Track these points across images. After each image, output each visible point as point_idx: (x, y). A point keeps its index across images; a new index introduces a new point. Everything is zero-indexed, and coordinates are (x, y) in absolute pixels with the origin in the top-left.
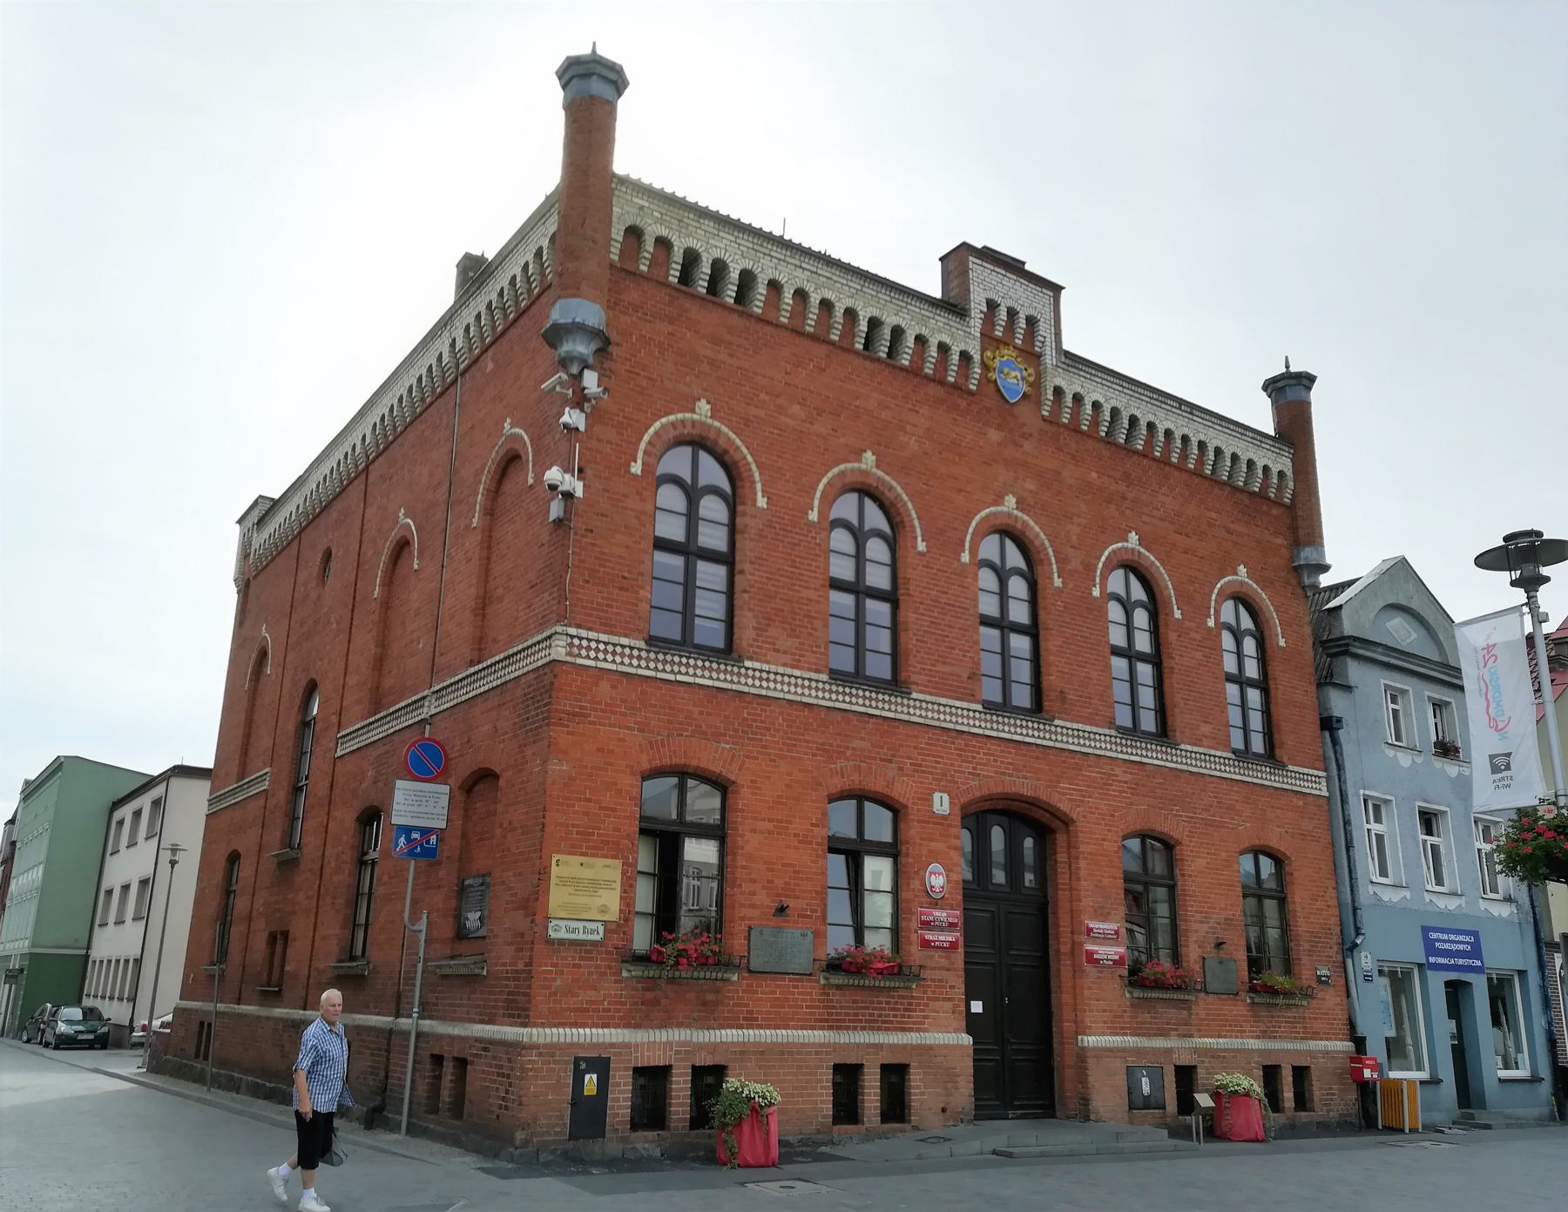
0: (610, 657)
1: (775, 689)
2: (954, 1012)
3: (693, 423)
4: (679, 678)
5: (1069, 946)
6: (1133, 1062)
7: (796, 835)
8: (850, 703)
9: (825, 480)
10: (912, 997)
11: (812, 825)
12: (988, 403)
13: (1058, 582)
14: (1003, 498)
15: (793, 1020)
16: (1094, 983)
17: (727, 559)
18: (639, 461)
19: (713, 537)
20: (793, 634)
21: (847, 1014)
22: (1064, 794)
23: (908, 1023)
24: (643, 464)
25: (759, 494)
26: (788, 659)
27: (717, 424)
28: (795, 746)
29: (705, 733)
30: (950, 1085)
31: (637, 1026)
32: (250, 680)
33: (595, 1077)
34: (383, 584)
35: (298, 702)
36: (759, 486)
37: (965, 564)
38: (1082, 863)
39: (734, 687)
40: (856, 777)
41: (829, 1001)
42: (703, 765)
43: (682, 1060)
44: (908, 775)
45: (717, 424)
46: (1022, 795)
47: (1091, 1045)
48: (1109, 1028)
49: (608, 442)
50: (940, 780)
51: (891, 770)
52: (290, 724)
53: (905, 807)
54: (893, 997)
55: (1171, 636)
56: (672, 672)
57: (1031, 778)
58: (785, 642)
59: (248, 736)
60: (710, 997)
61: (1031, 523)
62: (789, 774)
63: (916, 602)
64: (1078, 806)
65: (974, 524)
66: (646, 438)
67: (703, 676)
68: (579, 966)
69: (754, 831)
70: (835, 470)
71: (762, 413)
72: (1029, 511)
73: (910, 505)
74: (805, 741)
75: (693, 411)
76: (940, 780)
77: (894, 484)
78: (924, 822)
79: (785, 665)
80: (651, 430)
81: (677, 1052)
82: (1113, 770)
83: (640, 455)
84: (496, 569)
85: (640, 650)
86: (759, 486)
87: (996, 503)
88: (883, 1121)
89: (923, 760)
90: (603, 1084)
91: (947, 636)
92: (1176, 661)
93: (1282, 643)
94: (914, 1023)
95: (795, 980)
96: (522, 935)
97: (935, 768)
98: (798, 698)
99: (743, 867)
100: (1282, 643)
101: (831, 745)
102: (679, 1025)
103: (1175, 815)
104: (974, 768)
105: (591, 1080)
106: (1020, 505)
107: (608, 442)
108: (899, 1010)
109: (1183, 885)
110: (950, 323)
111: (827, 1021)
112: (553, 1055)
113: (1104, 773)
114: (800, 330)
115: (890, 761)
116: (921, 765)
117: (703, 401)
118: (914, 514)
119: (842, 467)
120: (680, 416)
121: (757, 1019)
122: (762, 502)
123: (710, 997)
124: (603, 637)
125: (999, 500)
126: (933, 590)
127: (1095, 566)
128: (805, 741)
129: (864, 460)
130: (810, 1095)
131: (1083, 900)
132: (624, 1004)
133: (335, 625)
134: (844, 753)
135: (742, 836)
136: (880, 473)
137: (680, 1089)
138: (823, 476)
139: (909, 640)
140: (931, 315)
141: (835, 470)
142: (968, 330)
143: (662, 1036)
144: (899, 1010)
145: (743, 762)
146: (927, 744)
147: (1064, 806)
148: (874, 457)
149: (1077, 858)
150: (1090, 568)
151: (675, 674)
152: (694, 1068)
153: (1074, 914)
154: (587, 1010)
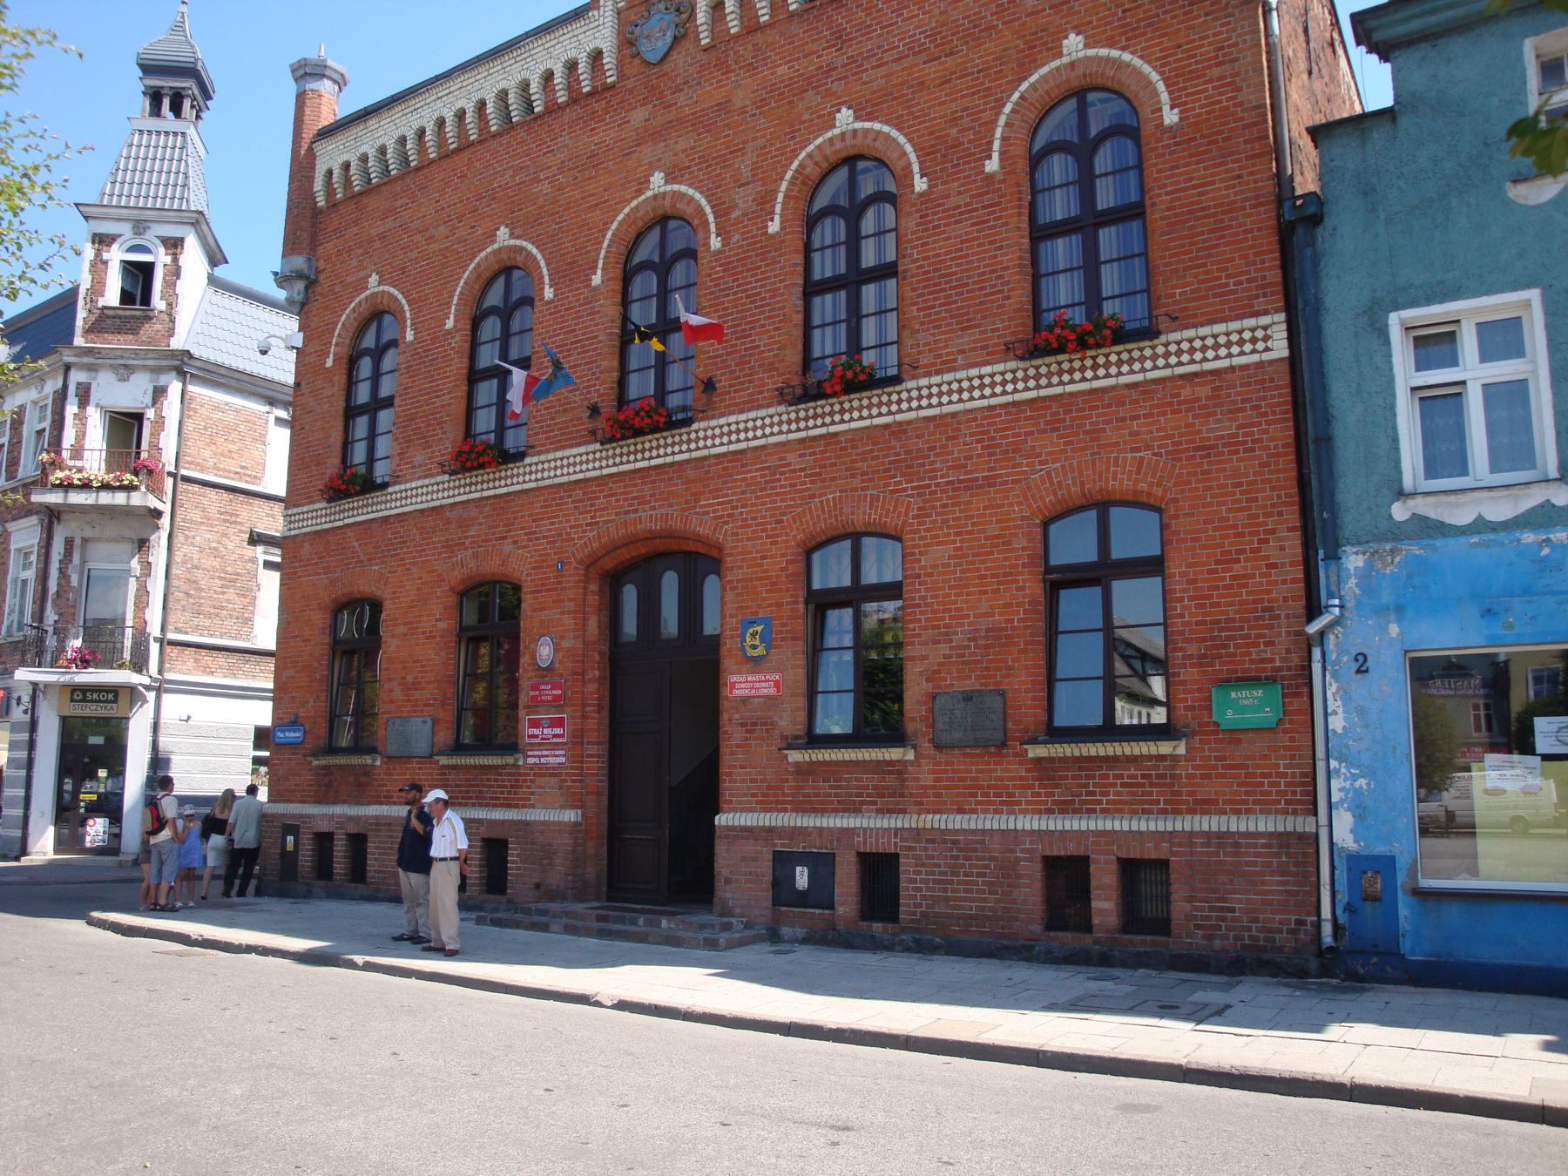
2: (561, 788)
6: (783, 845)
7: (424, 633)
11: (437, 620)
13: (715, 243)
16: (737, 746)
21: (461, 792)
22: (707, 513)
23: (513, 799)
30: (545, 862)
37: (596, 288)
40: (473, 565)
46: (651, 531)
47: (724, 823)
48: (758, 802)
50: (555, 542)
51: (508, 547)
54: (501, 774)
60: (363, 779)
62: (420, 578)
64: (727, 523)
69: (393, 637)
76: (555, 542)
79: (419, 478)
82: (781, 459)
87: (640, 192)
89: (537, 526)
94: (520, 799)
95: (421, 763)
97: (550, 530)
100: (1170, 117)
103: (892, 492)
104: (592, 518)
105: (290, 839)
106: (670, 178)
108: (506, 786)
109: (796, 603)
113: (769, 468)
116: (535, 532)
118: (542, 263)
123: (363, 779)
134: (464, 543)
138: (460, 278)
143: (339, 809)
144: (506, 786)
146: (542, 507)
147: (704, 530)
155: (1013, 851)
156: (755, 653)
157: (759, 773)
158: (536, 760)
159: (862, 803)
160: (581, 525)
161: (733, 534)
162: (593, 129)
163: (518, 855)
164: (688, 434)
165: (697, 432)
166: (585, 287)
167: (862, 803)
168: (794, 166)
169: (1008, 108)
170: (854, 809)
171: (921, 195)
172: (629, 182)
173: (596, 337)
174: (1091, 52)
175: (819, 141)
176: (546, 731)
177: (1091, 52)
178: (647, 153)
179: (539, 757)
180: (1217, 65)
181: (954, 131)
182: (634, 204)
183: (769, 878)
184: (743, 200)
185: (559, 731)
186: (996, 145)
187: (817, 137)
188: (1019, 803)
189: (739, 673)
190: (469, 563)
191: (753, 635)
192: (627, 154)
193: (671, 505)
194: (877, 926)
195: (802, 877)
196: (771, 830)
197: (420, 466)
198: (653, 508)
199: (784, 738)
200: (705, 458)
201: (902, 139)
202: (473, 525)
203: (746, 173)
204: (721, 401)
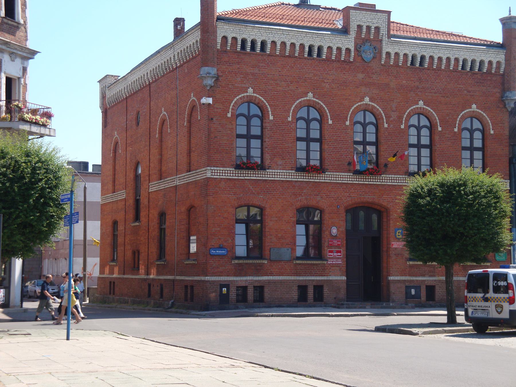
0: (224, 174)
1: (277, 177)
2: (340, 270)
3: (247, 96)
4: (246, 178)
5: (386, 249)
8: (303, 178)
9: (294, 106)
10: (325, 266)
11: (290, 217)
12: (358, 64)
13: (386, 125)
14: (364, 98)
15: (285, 273)
17: (261, 137)
18: (230, 113)
19: (256, 131)
20: (283, 159)
22: (385, 199)
24: (231, 113)
25: (270, 115)
26: (280, 167)
27: (255, 95)
28: (284, 194)
29: (254, 193)
30: (337, 291)
31: (237, 276)
32: (113, 153)
33: (226, 289)
34: (159, 133)
35: (133, 167)
36: (270, 113)
37: (347, 126)
38: (391, 222)
39: (263, 178)
40: (305, 202)
41: (296, 268)
42: (254, 202)
43: (250, 284)
44: (324, 199)
45: (255, 95)
49: (220, 108)
50: (336, 199)
51: (319, 198)
52: (131, 176)
53: (324, 209)
54: (318, 266)
55: (436, 138)
56: (243, 176)
57: (371, 195)
58: (280, 162)
59: (114, 175)
61: (376, 105)
63: (328, 141)
64: (391, 203)
65: (351, 110)
66: (232, 104)
67: (253, 176)
68: (220, 261)
70: (298, 102)
71: (270, 87)
72: (375, 101)
73: (326, 108)
74: (288, 192)
75: (247, 92)
76: (336, 199)
77: (320, 102)
78: (330, 213)
79: (280, 169)
80: (234, 102)
81: (249, 282)
83: (230, 110)
84: (192, 141)
85: (233, 171)
86: (270, 113)
87: (361, 101)
88: (314, 301)
89: (330, 194)
90: (228, 291)
91: (340, 152)
92: (437, 147)
93: (492, 132)
94: (325, 273)
95: (286, 262)
96: (204, 253)
98: (285, 179)
99: (268, 231)
100: (492, 132)
101: (297, 192)
102: (250, 275)
106: (371, 100)
107: (220, 108)
108: (320, 270)
110: (342, 39)
111: (296, 273)
112: (214, 283)
114: (284, 55)
115: (318, 195)
116: (329, 195)
117: (250, 88)
118: (327, 111)
119: (300, 100)
120: (243, 95)
121: (273, 273)
122: (271, 118)
124: (222, 169)
125: (362, 99)
126: (335, 136)
127: (403, 117)
128: (288, 192)
129: (308, 96)
130: (290, 294)
131: (391, 233)
132: (232, 270)
133: (144, 143)
134: (301, 194)
135: (267, 222)
136: (315, 99)
137: (250, 292)
138: (293, 104)
139: (326, 155)
140: (334, 38)
141: (298, 102)
142: (349, 40)
143: (244, 278)
145: (267, 201)
147: (385, 204)
148: (312, 94)
149: (389, 220)
150: (400, 118)
151: (244, 177)
152: (254, 287)
153: (388, 238)
154: (223, 272)
155: (460, 284)
156: (399, 237)
157: (400, 267)
158: (330, 262)
159: (426, 274)
160: (345, 196)
161: (392, 206)
162: (345, 73)
163: (327, 290)
164: (380, 177)
165: (382, 177)
166: (344, 124)
167: (426, 274)
168: (408, 111)
169: (460, 117)
170: (423, 275)
171: (440, 131)
172: (358, 96)
173: (348, 141)
174: (478, 110)
175: (414, 107)
176: (335, 254)
177: (478, 110)
178: (363, 89)
179: (333, 261)
180: (501, 123)
181: (448, 118)
182: (359, 104)
183: (405, 292)
184: (394, 116)
185: (339, 254)
186: (457, 125)
187: (414, 105)
188: (459, 274)
189: (394, 242)
190: (302, 201)
191: (399, 232)
192: (357, 87)
193: (375, 195)
194: (431, 302)
195: (413, 292)
196: (405, 281)
197: (280, 165)
198: (369, 195)
199: (406, 258)
200: (385, 185)
201: (436, 115)
202: (305, 189)
203: (394, 109)
204: (389, 170)
